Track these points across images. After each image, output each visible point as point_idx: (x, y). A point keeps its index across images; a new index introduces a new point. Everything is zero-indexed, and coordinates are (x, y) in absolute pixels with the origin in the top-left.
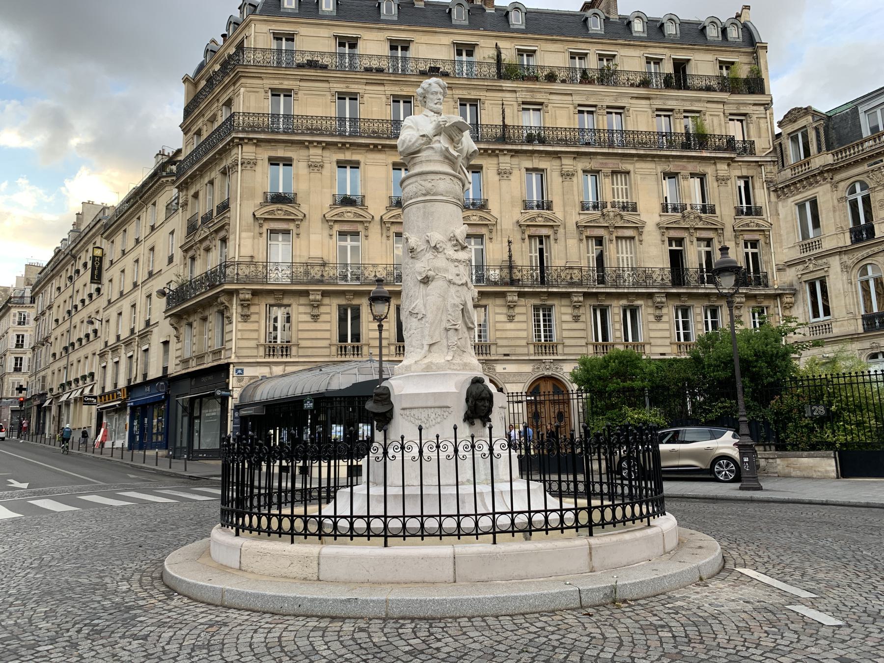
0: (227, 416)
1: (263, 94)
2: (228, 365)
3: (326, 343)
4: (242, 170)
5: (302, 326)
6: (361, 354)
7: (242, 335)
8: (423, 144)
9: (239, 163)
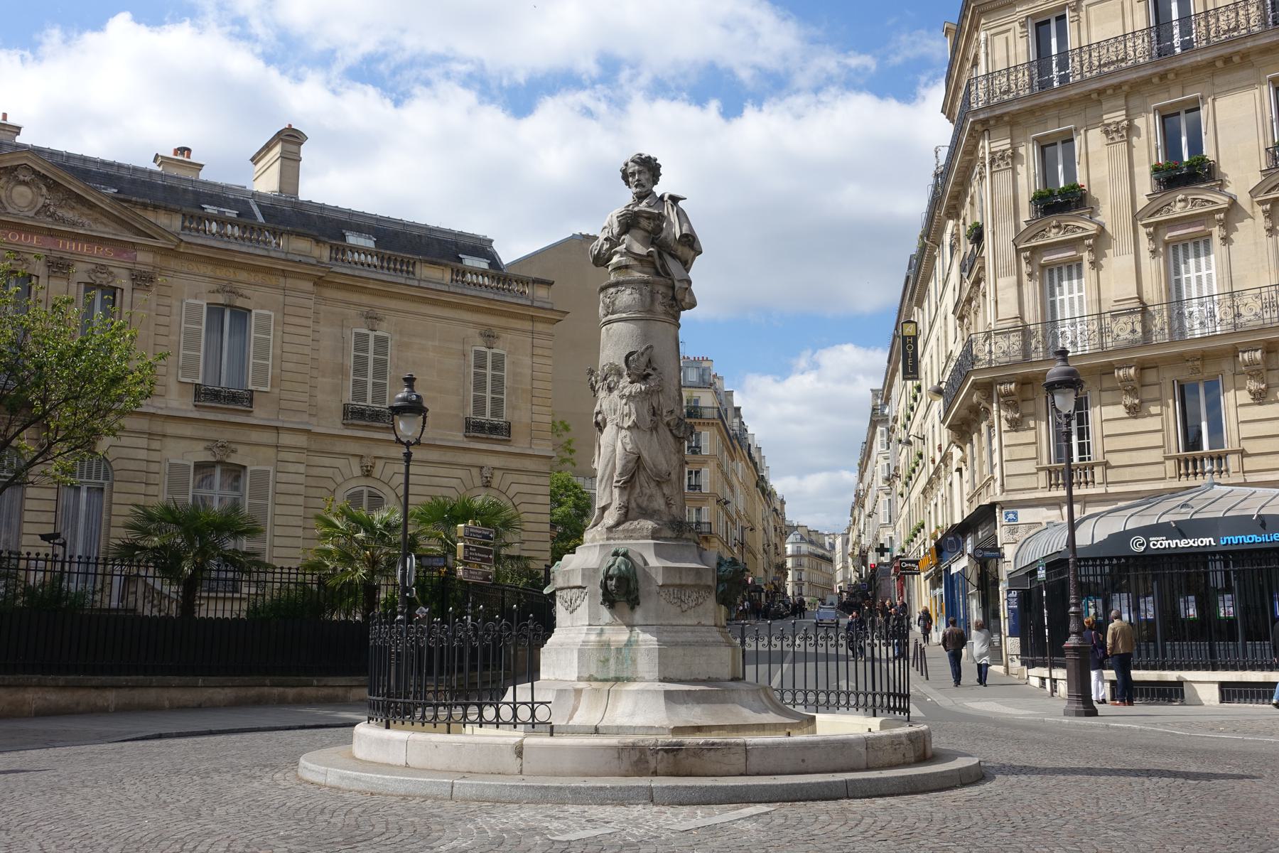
0: (998, 591)
1: (1018, 29)
2: (992, 506)
3: (1157, 455)
4: (992, 174)
5: (1110, 428)
6: (1227, 470)
7: (1010, 454)
8: (611, 248)
9: (987, 161)
